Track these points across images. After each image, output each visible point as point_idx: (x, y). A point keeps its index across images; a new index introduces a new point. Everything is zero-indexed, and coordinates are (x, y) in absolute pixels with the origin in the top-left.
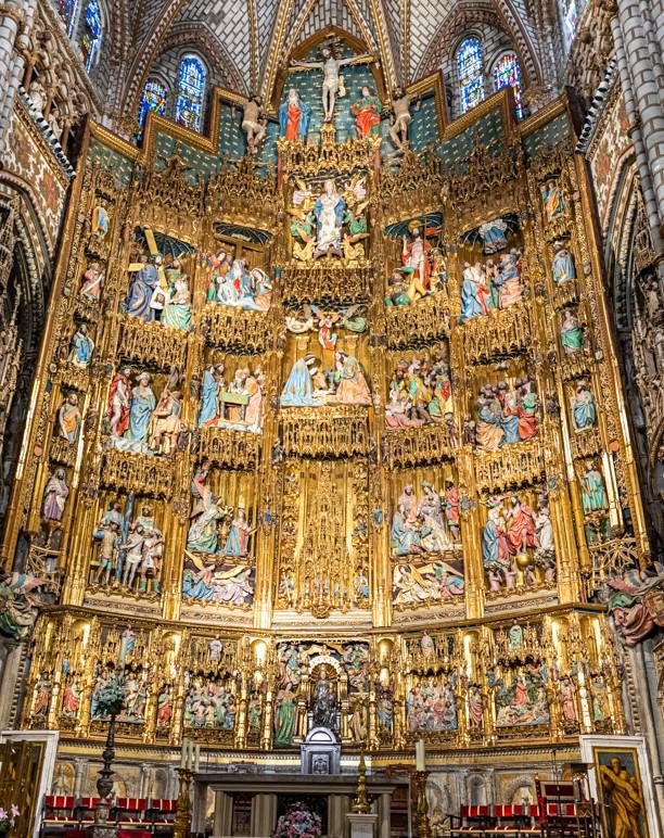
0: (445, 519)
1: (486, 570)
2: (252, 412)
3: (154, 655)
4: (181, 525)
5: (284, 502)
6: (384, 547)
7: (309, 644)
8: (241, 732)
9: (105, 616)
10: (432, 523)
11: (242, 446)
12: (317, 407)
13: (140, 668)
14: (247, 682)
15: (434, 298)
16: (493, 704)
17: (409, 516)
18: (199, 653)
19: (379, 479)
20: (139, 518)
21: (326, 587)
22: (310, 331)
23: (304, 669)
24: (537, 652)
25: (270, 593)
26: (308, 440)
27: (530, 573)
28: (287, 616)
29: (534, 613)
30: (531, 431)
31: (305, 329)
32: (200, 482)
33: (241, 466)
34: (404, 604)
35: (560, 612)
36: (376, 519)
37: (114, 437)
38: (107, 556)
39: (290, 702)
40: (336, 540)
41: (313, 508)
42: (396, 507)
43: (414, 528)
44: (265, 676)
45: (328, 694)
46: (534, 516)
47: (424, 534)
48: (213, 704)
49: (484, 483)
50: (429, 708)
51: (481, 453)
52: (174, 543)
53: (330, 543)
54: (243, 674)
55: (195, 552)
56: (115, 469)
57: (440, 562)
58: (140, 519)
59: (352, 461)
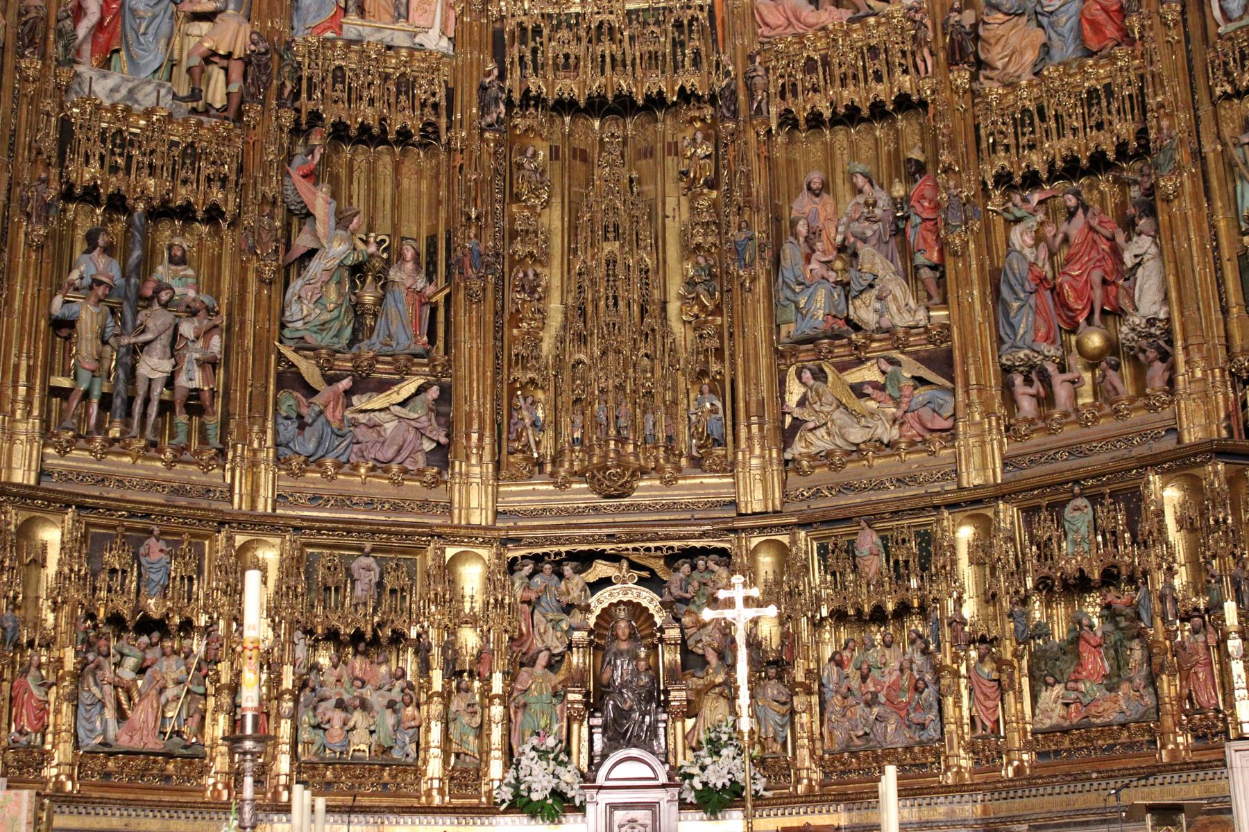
0: (907, 253)
1: (1007, 370)
3: (218, 595)
4: (262, 281)
5: (512, 220)
6: (762, 323)
7: (584, 560)
8: (434, 767)
9: (94, 508)
10: (874, 260)
11: (406, 85)
13: (187, 626)
14: (444, 653)
16: (1025, 682)
17: (819, 245)
18: (327, 589)
19: (742, 158)
20: (160, 268)
21: (622, 422)
23: (577, 618)
24: (1127, 555)
25: (487, 441)
26: (567, 64)
27: (1111, 373)
29: (1119, 472)
30: (1111, 31)
32: (304, 176)
33: (404, 135)
35: (1180, 463)
36: (738, 252)
37: (86, 69)
38: (89, 364)
39: (547, 693)
40: (643, 311)
42: (786, 224)
43: (832, 276)
44: (484, 637)
45: (636, 673)
46: (1120, 238)
47: (855, 287)
48: (364, 706)
49: (1001, 161)
50: (875, 695)
51: (993, 90)
52: (250, 330)
53: (628, 314)
54: (433, 633)
55: (301, 346)
56: (98, 149)
57: (895, 354)
58: (163, 271)
59: (675, 116)
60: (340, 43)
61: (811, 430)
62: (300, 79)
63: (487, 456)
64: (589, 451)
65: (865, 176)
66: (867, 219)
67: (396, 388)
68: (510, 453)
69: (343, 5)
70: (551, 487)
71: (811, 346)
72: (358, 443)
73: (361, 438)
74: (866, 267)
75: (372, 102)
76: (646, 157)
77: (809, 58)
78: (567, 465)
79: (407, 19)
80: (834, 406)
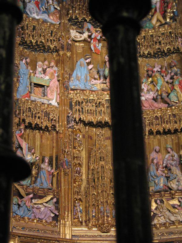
2: (52, 92)
11: (47, 114)
12: (94, 91)
15: (169, 25)
22: (85, 41)
25: (70, 215)
28: (82, 230)
31: (82, 38)
34: (160, 224)
41: (92, 159)
43: (164, 174)
60: (30, 101)
61: (159, 217)
62: (20, 110)
63: (70, 220)
64: (98, 220)
65: (171, 148)
66: (172, 160)
67: (45, 198)
68: (74, 219)
69: (30, 91)
70: (87, 229)
71: (159, 193)
72: (34, 213)
73: (35, 212)
74: (175, 173)
75: (39, 118)
76: (108, 139)
77: (156, 116)
78: (91, 223)
79: (47, 96)
80: (166, 210)
